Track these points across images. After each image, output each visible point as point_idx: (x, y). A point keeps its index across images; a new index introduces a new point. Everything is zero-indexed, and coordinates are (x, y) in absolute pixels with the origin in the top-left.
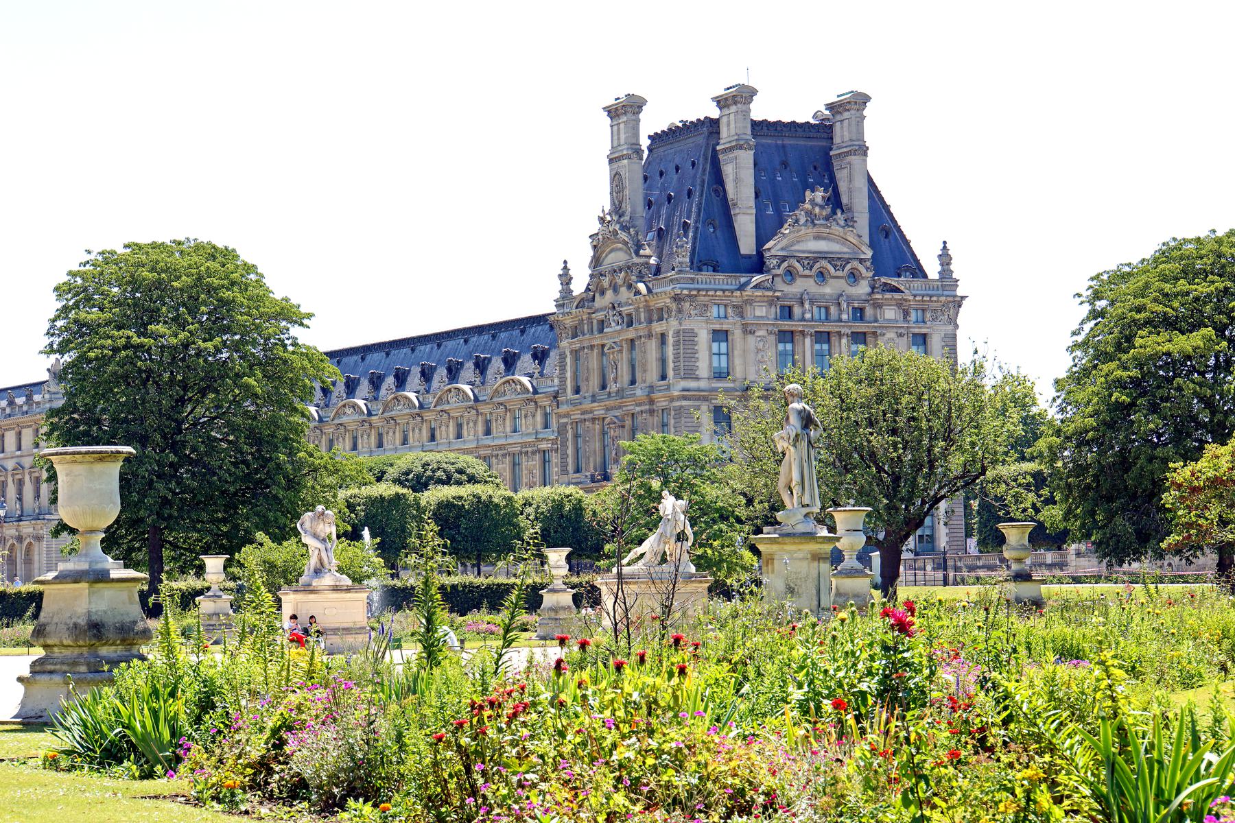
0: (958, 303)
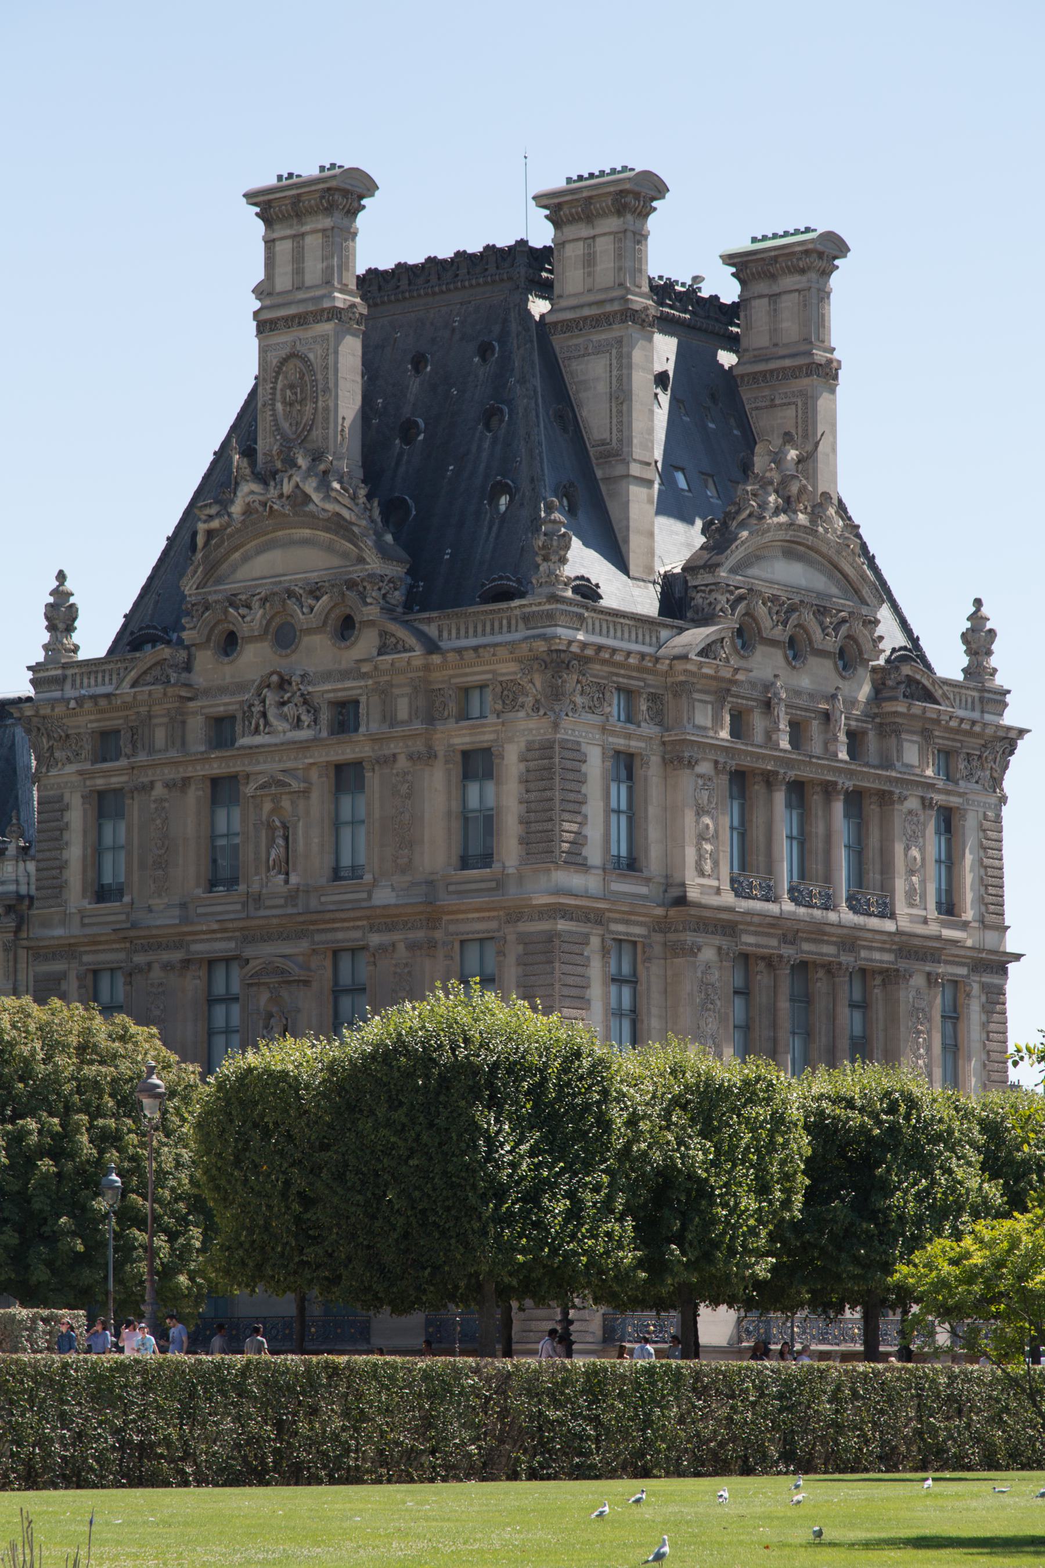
0: (1008, 741)
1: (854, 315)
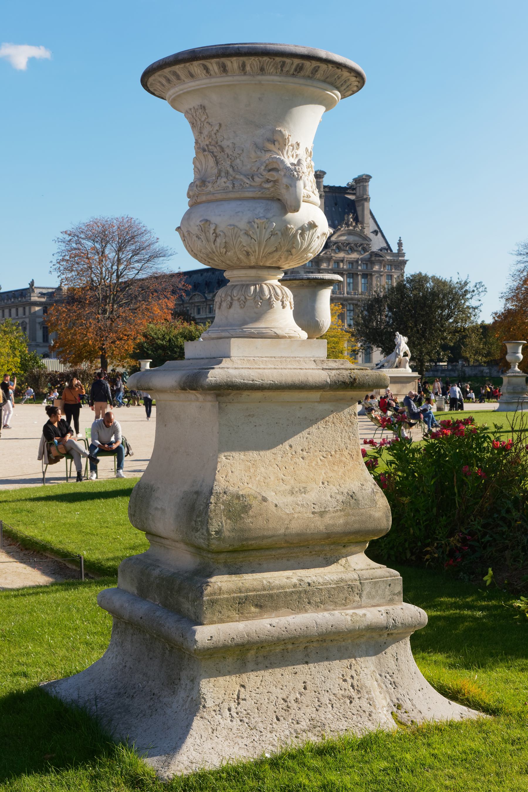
0: (404, 262)
1: (372, 189)
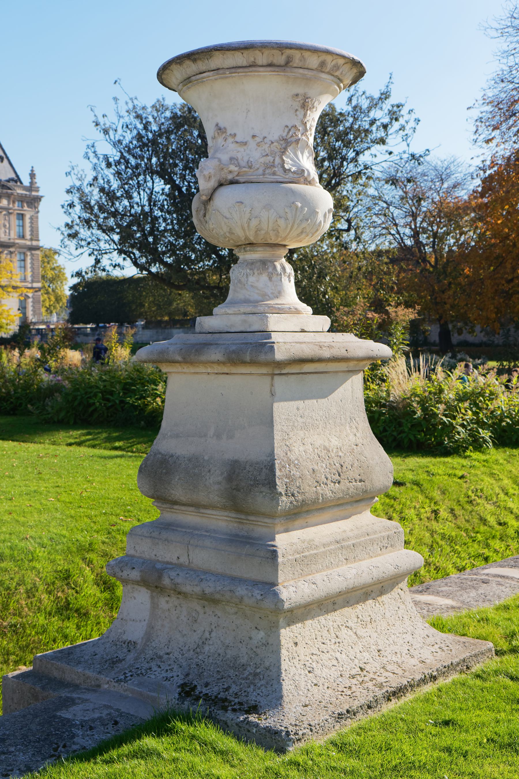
0: (38, 199)
